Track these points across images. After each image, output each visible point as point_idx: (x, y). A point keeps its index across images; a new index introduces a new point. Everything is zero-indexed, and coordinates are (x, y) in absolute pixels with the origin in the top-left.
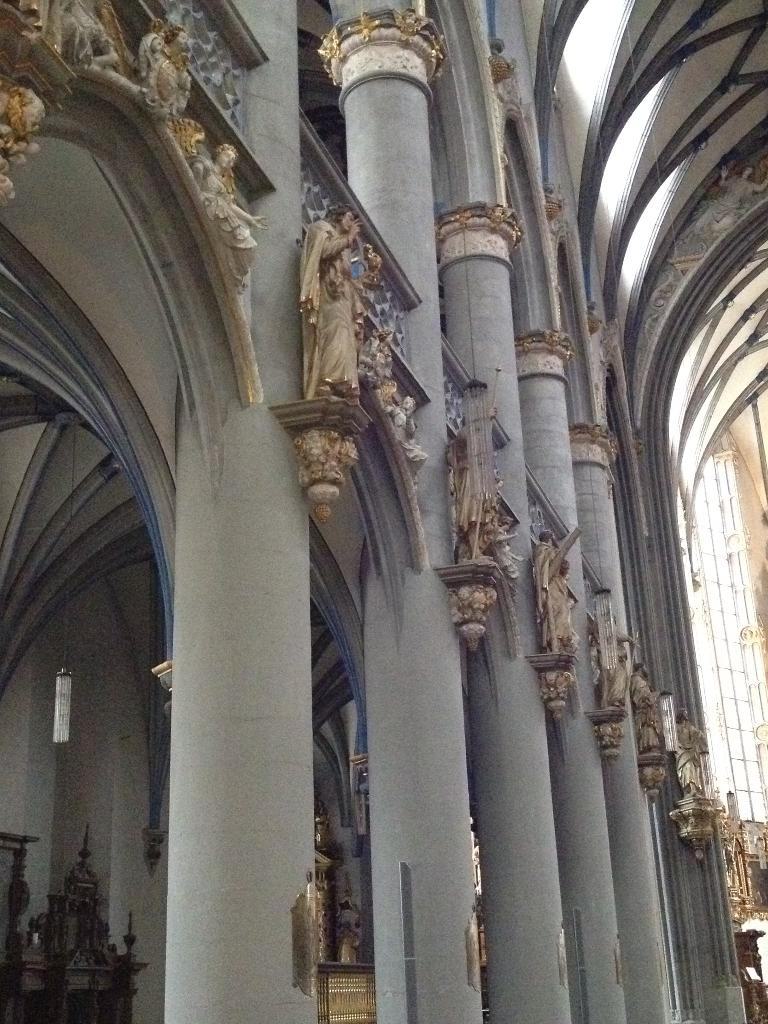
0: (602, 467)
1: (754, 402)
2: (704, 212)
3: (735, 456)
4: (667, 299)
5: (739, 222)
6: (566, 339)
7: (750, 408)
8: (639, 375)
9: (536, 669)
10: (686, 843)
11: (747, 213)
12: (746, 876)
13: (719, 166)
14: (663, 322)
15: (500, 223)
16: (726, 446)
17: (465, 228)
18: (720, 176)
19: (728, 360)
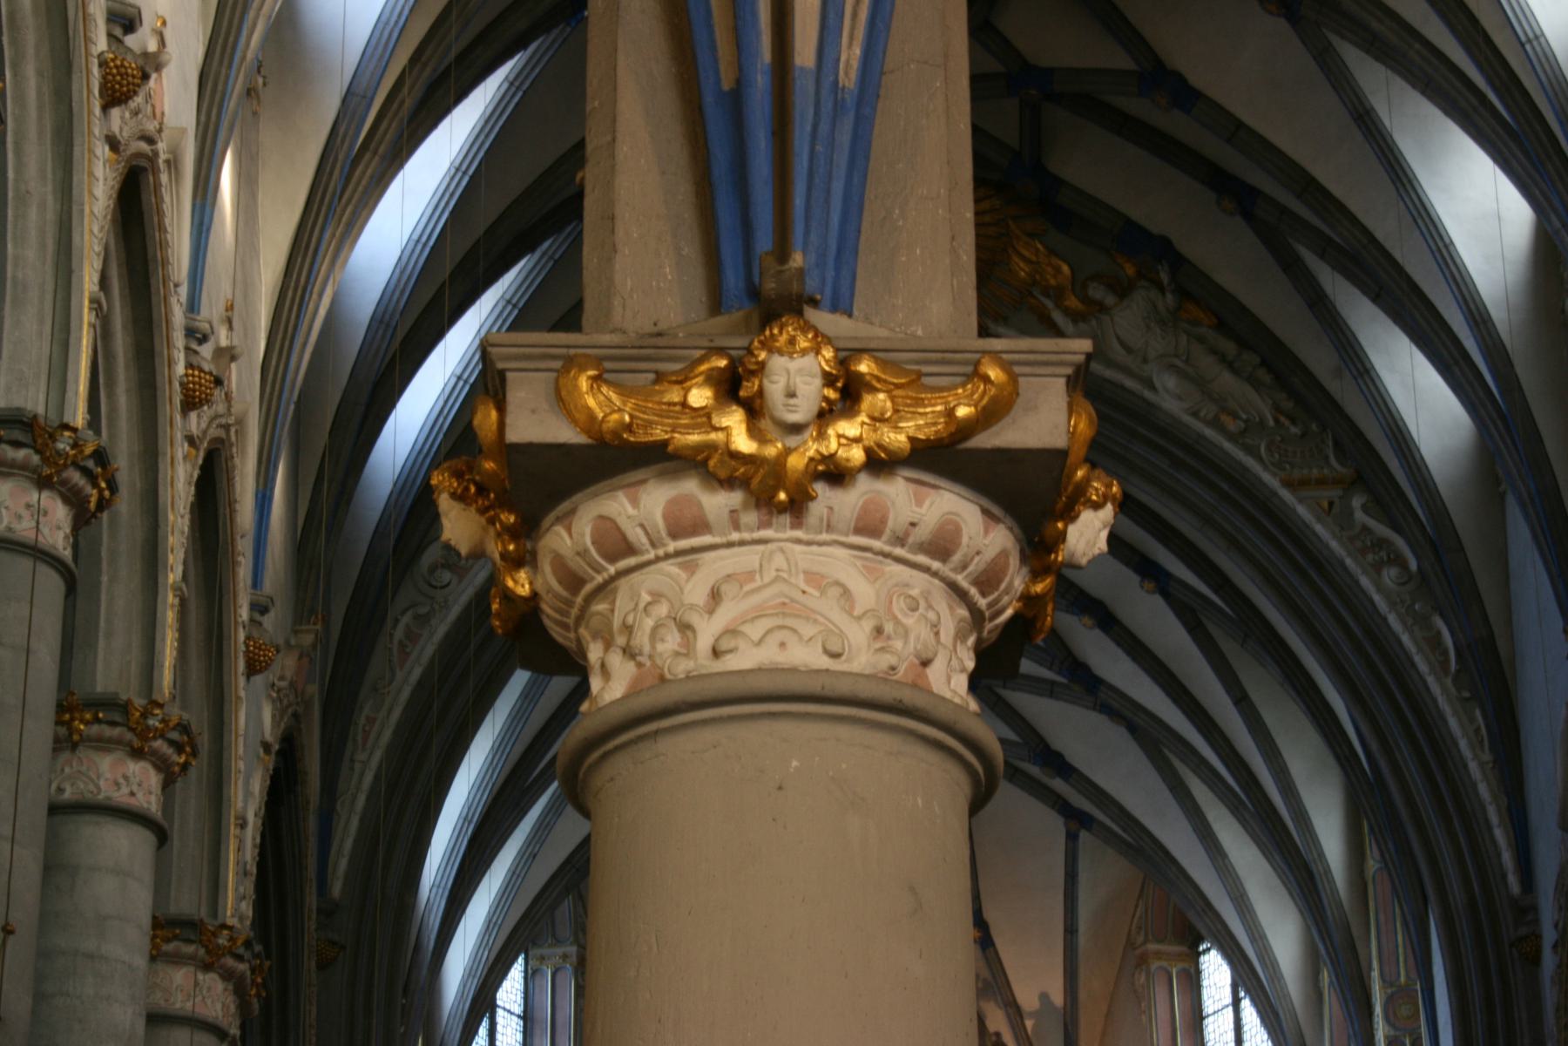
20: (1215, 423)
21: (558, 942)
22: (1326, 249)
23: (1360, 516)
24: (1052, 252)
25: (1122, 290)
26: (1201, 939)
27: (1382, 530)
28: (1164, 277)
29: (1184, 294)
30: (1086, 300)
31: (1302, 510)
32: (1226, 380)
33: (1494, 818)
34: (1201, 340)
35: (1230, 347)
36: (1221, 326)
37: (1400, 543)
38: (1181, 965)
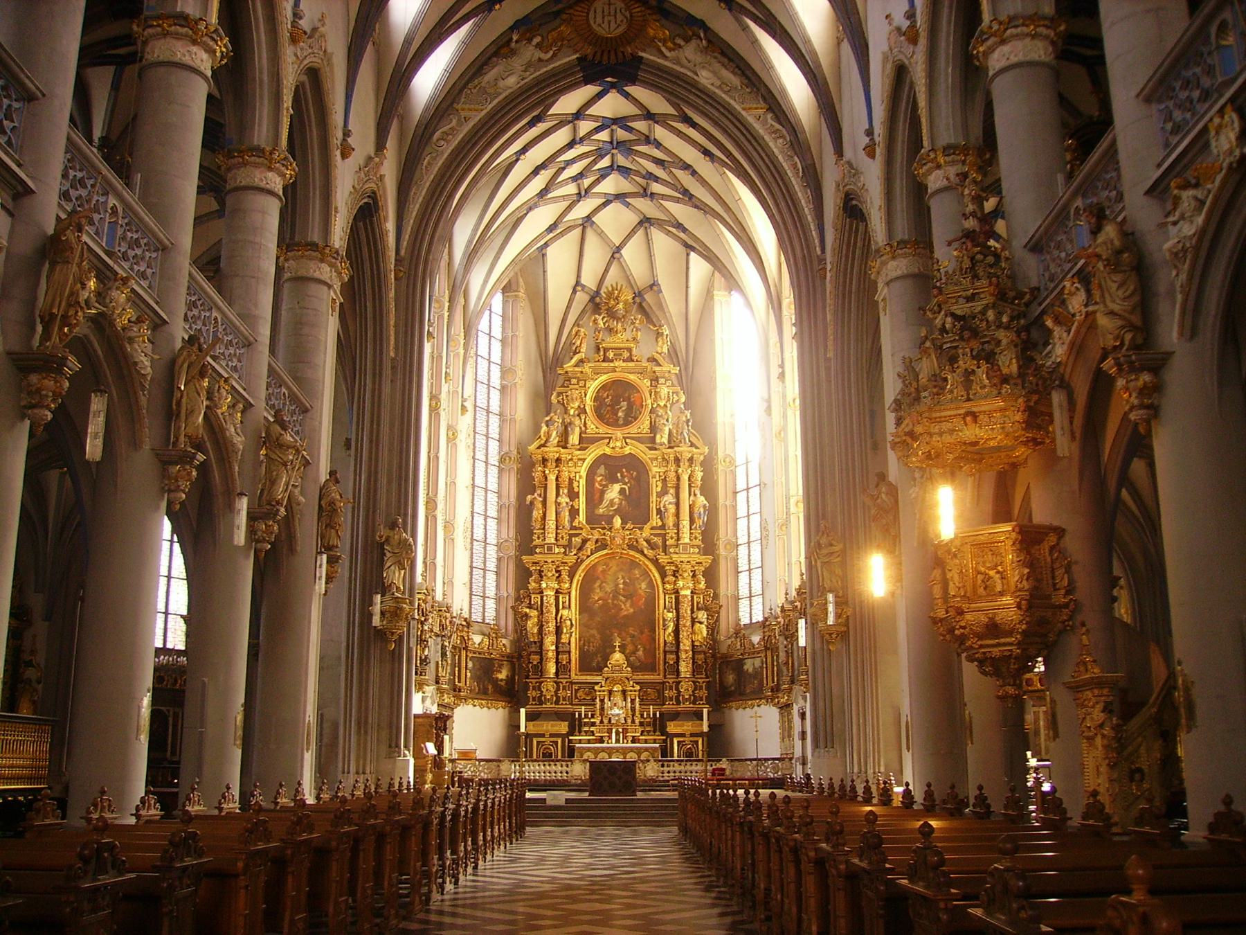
2: (493, 68)
4: (448, 142)
5: (523, 82)
9: (161, 461)
11: (531, 77)
13: (512, 29)
15: (202, 36)
17: (166, 34)
18: (511, 39)
20: (720, 87)
22: (756, 20)
23: (770, 121)
24: (662, 26)
25: (687, 40)
27: (778, 126)
28: (702, 35)
29: (709, 41)
30: (675, 44)
31: (751, 119)
32: (726, 74)
34: (715, 58)
35: (726, 61)
36: (723, 53)
37: (784, 130)
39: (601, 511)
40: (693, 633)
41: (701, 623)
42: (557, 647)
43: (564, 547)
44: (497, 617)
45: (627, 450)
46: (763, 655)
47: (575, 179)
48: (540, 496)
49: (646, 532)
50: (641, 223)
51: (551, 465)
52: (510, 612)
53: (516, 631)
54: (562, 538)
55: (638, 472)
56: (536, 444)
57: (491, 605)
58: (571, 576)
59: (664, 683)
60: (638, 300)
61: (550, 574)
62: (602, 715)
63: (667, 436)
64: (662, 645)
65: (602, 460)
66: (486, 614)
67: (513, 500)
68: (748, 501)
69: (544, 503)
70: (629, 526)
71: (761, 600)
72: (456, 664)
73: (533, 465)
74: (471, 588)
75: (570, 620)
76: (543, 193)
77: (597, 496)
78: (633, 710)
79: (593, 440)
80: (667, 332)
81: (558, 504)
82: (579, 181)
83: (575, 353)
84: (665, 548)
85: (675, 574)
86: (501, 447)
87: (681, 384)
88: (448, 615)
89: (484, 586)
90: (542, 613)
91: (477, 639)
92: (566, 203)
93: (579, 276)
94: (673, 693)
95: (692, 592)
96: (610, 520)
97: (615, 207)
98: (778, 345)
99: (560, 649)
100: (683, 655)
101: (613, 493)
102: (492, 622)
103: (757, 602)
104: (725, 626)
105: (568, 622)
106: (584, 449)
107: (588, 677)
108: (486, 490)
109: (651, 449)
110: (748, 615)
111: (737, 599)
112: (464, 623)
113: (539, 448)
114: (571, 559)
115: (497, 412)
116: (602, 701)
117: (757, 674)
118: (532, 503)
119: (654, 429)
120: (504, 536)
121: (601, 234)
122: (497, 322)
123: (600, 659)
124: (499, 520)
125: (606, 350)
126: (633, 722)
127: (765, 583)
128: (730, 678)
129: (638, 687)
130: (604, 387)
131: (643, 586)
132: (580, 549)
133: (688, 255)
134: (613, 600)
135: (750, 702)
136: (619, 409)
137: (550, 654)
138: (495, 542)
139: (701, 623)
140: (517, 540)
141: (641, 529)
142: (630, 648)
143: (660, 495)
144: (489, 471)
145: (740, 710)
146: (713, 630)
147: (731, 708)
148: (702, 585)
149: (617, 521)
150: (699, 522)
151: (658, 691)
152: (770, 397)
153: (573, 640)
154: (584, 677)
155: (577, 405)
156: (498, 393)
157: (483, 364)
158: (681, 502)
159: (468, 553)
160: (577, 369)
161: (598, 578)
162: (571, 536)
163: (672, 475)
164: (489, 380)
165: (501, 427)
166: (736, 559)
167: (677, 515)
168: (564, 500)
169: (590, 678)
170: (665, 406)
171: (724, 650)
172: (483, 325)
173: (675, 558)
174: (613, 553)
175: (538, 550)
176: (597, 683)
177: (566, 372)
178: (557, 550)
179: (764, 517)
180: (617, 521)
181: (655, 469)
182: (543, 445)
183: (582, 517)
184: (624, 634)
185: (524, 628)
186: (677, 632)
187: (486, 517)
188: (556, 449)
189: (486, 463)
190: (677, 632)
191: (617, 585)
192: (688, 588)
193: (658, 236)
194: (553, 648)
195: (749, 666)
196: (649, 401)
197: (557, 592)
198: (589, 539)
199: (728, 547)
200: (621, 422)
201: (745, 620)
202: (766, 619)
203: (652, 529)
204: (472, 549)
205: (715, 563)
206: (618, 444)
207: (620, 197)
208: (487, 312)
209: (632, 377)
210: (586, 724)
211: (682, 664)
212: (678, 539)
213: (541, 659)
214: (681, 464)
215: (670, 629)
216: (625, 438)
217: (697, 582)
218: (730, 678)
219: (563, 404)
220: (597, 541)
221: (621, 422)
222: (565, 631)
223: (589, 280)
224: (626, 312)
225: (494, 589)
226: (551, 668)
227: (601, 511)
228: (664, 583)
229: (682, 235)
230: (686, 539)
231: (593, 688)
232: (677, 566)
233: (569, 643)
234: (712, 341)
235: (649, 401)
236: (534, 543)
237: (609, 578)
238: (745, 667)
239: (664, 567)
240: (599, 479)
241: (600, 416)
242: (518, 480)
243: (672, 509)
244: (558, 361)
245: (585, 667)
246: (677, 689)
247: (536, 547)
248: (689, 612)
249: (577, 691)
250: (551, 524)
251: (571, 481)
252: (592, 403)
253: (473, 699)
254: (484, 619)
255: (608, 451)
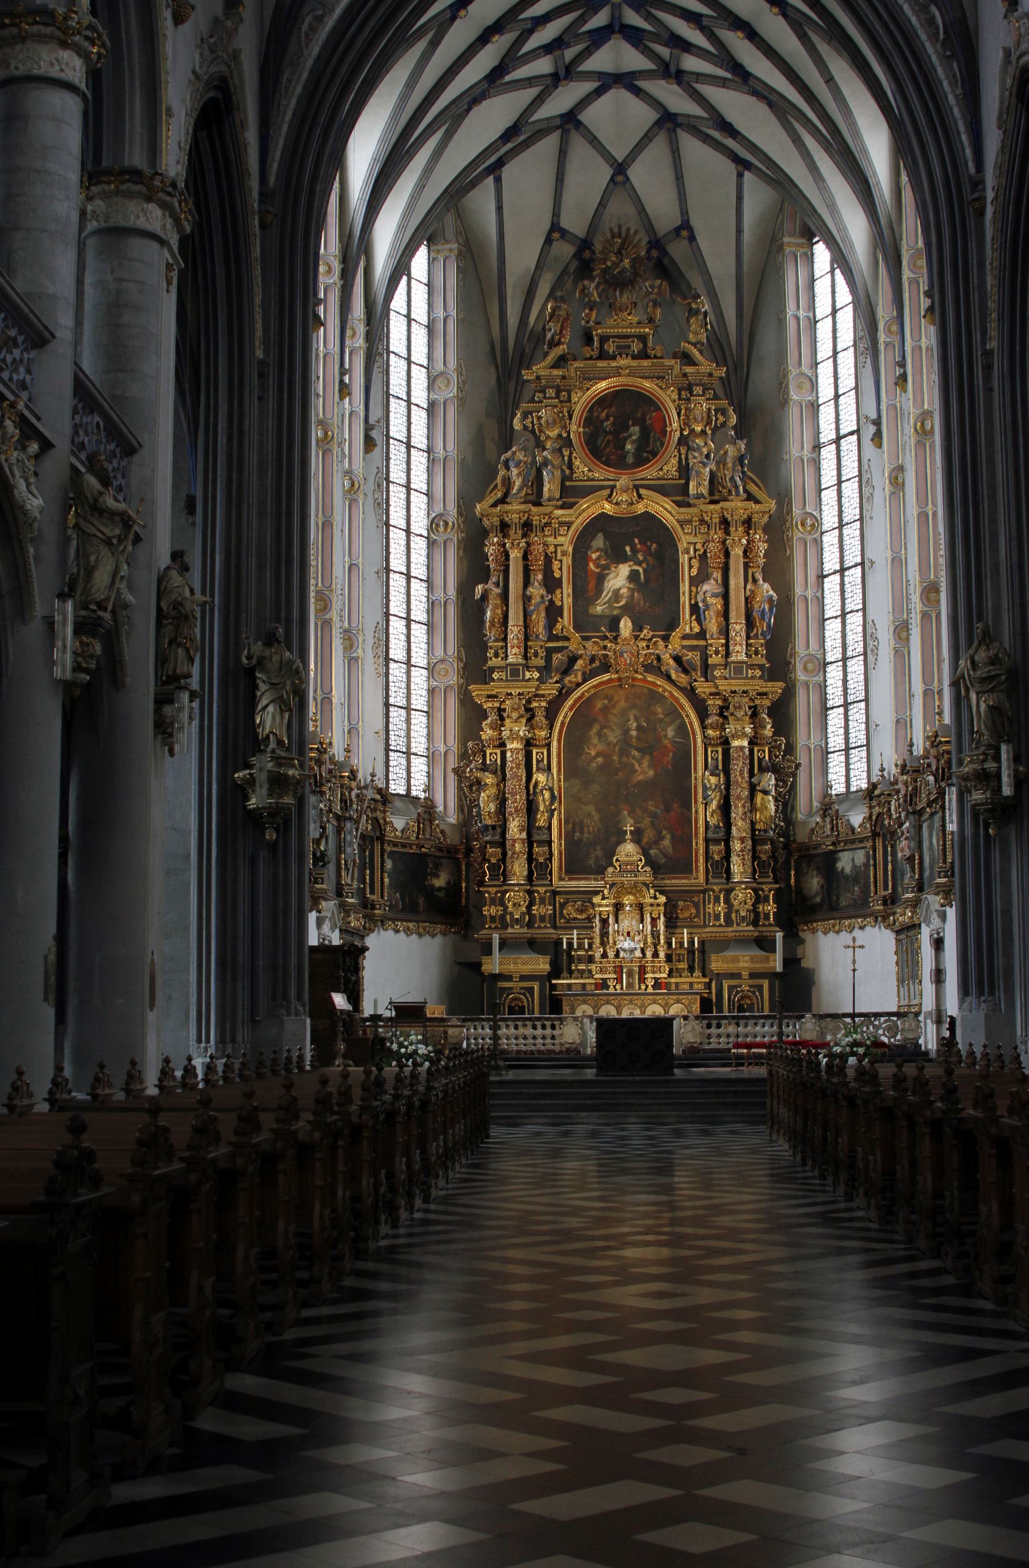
0: (162, 242)
1: (497, 173)
3: (460, 253)
6: (91, 27)
7: (490, 180)
8: (284, 102)
10: (254, 818)
12: (382, 872)
14: (330, 23)
16: (450, 233)
19: (453, 102)
21: (447, 242)
26: (814, 235)
33: (962, 129)
38: (802, 250)
39: (599, 608)
40: (753, 809)
41: (766, 793)
42: (529, 835)
43: (539, 669)
44: (428, 789)
45: (640, 508)
46: (869, 844)
47: (548, 49)
48: (497, 585)
49: (676, 643)
50: (658, 124)
51: (516, 533)
52: (452, 778)
53: (461, 808)
54: (536, 654)
55: (659, 545)
56: (491, 500)
57: (419, 766)
58: (551, 714)
59: (704, 892)
60: (655, 253)
61: (515, 715)
62: (603, 944)
63: (706, 483)
64: (702, 830)
65: (600, 523)
66: (413, 782)
67: (452, 592)
68: (843, 591)
69: (505, 596)
70: (646, 633)
71: (864, 754)
72: (366, 864)
73: (485, 533)
74: (387, 739)
75: (551, 790)
76: (495, 77)
77: (592, 584)
78: (655, 935)
79: (586, 492)
80: (706, 307)
81: (526, 599)
82: (558, 53)
83: (553, 344)
84: (706, 669)
85: (722, 711)
86: (430, 506)
87: (729, 396)
88: (354, 784)
89: (408, 736)
90: (504, 778)
91: (399, 823)
92: (533, 92)
93: (556, 214)
94: (721, 908)
95: (750, 743)
96: (614, 624)
97: (617, 97)
98: (895, 328)
99: (536, 837)
100: (736, 846)
101: (619, 578)
102: (422, 795)
103: (858, 756)
104: (807, 802)
105: (547, 795)
106: (570, 506)
107: (582, 883)
108: (408, 577)
109: (679, 504)
110: (843, 779)
111: (825, 753)
112: (378, 797)
113: (494, 505)
114: (550, 690)
115: (424, 447)
116: (604, 922)
117: (859, 876)
118: (485, 597)
119: (685, 471)
120: (439, 652)
121: (594, 141)
122: (420, 294)
123: (599, 852)
124: (430, 625)
125: (604, 339)
126: (656, 955)
127: (872, 727)
128: (814, 883)
129: (662, 899)
130: (603, 401)
131: (670, 732)
132: (566, 671)
133: (740, 175)
134: (620, 756)
135: (847, 922)
136: (625, 439)
137: (518, 847)
138: (423, 663)
139: (766, 793)
140: (460, 659)
141: (666, 639)
142: (649, 834)
143: (696, 582)
144: (412, 545)
145: (831, 935)
146: (785, 805)
147: (814, 931)
148: (768, 731)
149: (626, 626)
150: (761, 627)
151: (696, 905)
152: (879, 416)
153: (555, 822)
154: (573, 883)
155: (556, 432)
156: (424, 414)
157: (397, 368)
158: (732, 593)
159: (382, 681)
160: (555, 372)
161: (595, 720)
162: (550, 652)
163: (714, 548)
164: (409, 393)
165: (430, 471)
166: (823, 687)
167: (726, 614)
168: (536, 591)
169: (582, 884)
170: (703, 432)
171: (801, 836)
172: (398, 302)
173: (723, 686)
174: (619, 679)
175: (495, 676)
176: (597, 893)
177: (538, 378)
178: (528, 675)
179: (869, 620)
180: (626, 626)
181: (686, 541)
182: (503, 501)
183: (566, 622)
184: (638, 811)
185: (474, 803)
186: (725, 808)
187: (409, 621)
188: (523, 507)
189: (408, 532)
190: (725, 808)
191: (626, 732)
192: (744, 735)
193: (691, 146)
194: (524, 835)
195: (845, 862)
196: (675, 425)
197: (529, 744)
198: (581, 656)
199: (810, 666)
200: (630, 460)
201: (838, 787)
202: (873, 786)
203: (685, 637)
204: (387, 675)
205: (789, 693)
206: (624, 497)
207: (626, 80)
208: (405, 278)
209: (647, 384)
210: (580, 959)
211: (734, 859)
212: (728, 654)
213: (504, 854)
214: (732, 529)
215: (714, 805)
216: (637, 488)
217: (758, 726)
218: (814, 883)
219: (533, 431)
220: (593, 659)
221: (630, 460)
222: (542, 808)
223: (575, 222)
224: (636, 274)
225: (424, 740)
226: (519, 869)
227: (599, 608)
228: (704, 727)
229: (730, 143)
230: (739, 654)
231: (590, 901)
232: (725, 700)
233: (550, 828)
234: (781, 322)
235: (675, 425)
236: (490, 663)
237: (611, 717)
238: (839, 865)
239: (704, 701)
240: (594, 556)
241: (596, 451)
242: (460, 560)
243: (717, 604)
244: (524, 359)
245: (574, 867)
246: (727, 901)
247: (492, 670)
248: (746, 775)
249: (563, 906)
250: (515, 631)
251: (548, 560)
252: (581, 430)
253: (393, 920)
254: (409, 789)
255: (608, 508)
